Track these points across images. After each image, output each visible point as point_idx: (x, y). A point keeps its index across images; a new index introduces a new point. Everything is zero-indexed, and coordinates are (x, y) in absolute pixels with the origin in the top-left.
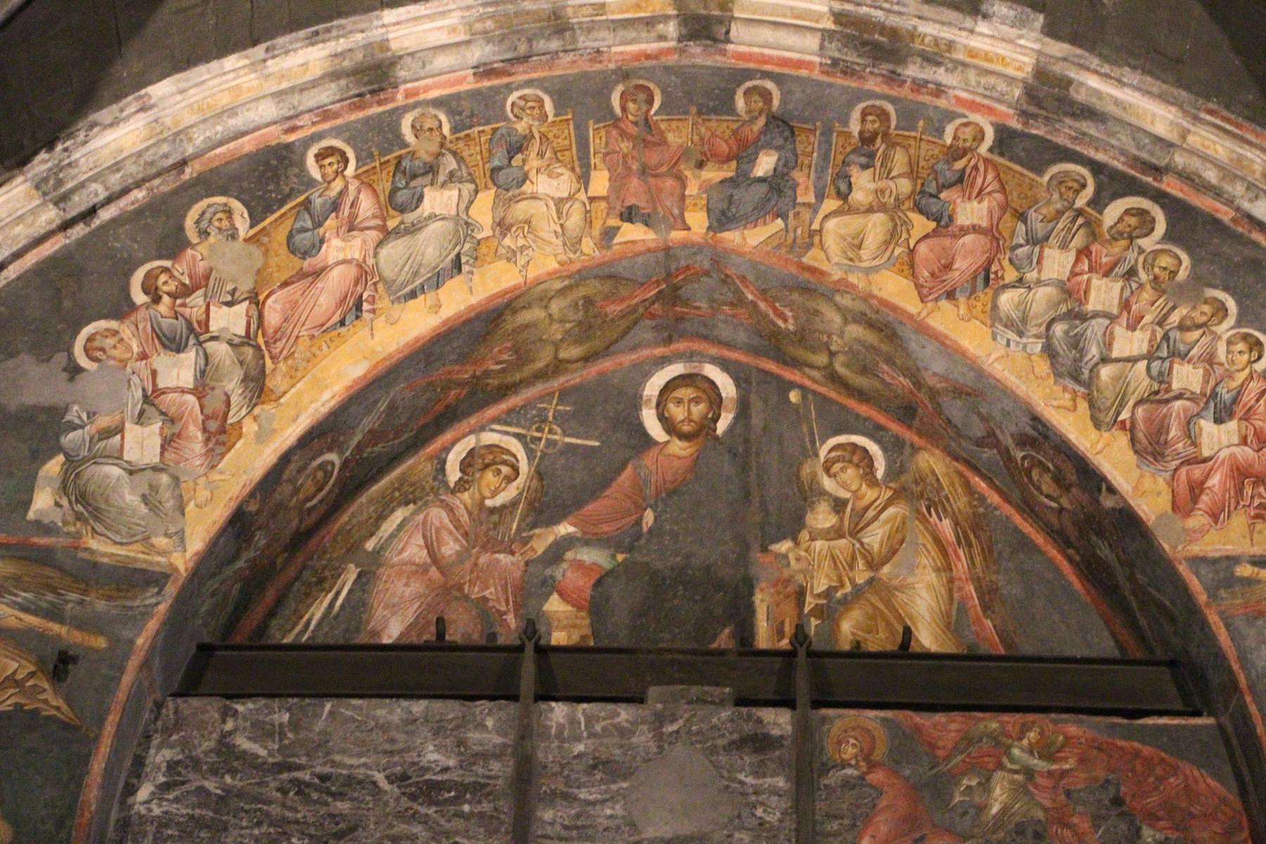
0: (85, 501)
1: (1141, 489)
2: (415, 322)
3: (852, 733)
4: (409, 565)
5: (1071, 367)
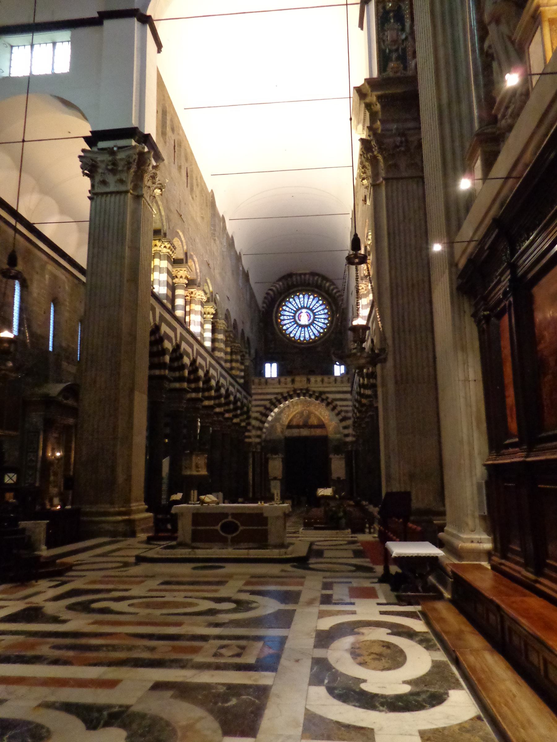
0: (283, 422)
1: (323, 420)
2: (294, 413)
3: (312, 430)
4: (294, 423)
5: (321, 414)
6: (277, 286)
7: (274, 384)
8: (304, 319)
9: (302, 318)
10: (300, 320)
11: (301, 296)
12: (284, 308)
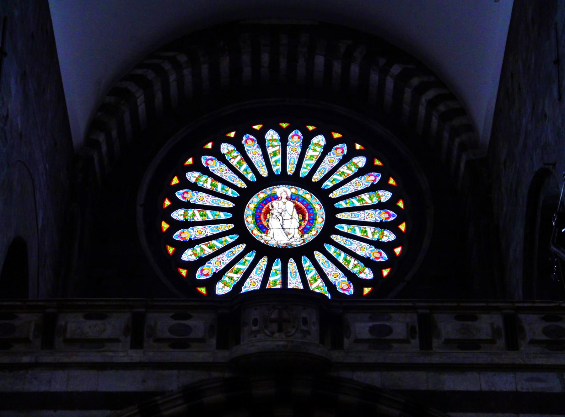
6: (167, 66)
7: (98, 343)
8: (284, 226)
9: (273, 223)
10: (264, 229)
11: (272, 135)
12: (192, 176)
